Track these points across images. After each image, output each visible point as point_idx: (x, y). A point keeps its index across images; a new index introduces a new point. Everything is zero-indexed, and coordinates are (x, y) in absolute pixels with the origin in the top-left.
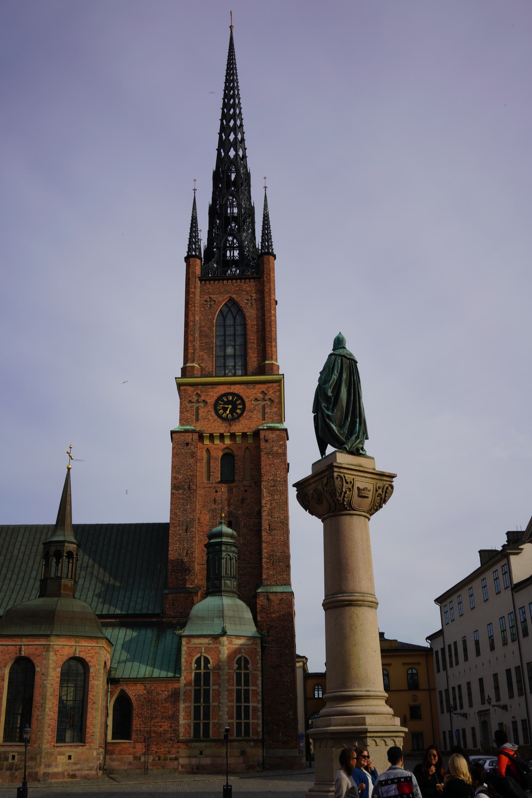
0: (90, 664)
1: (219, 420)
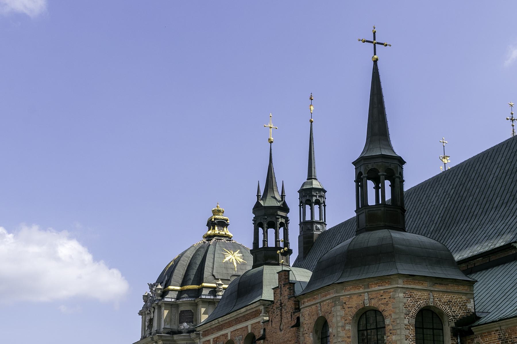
0: (385, 314)
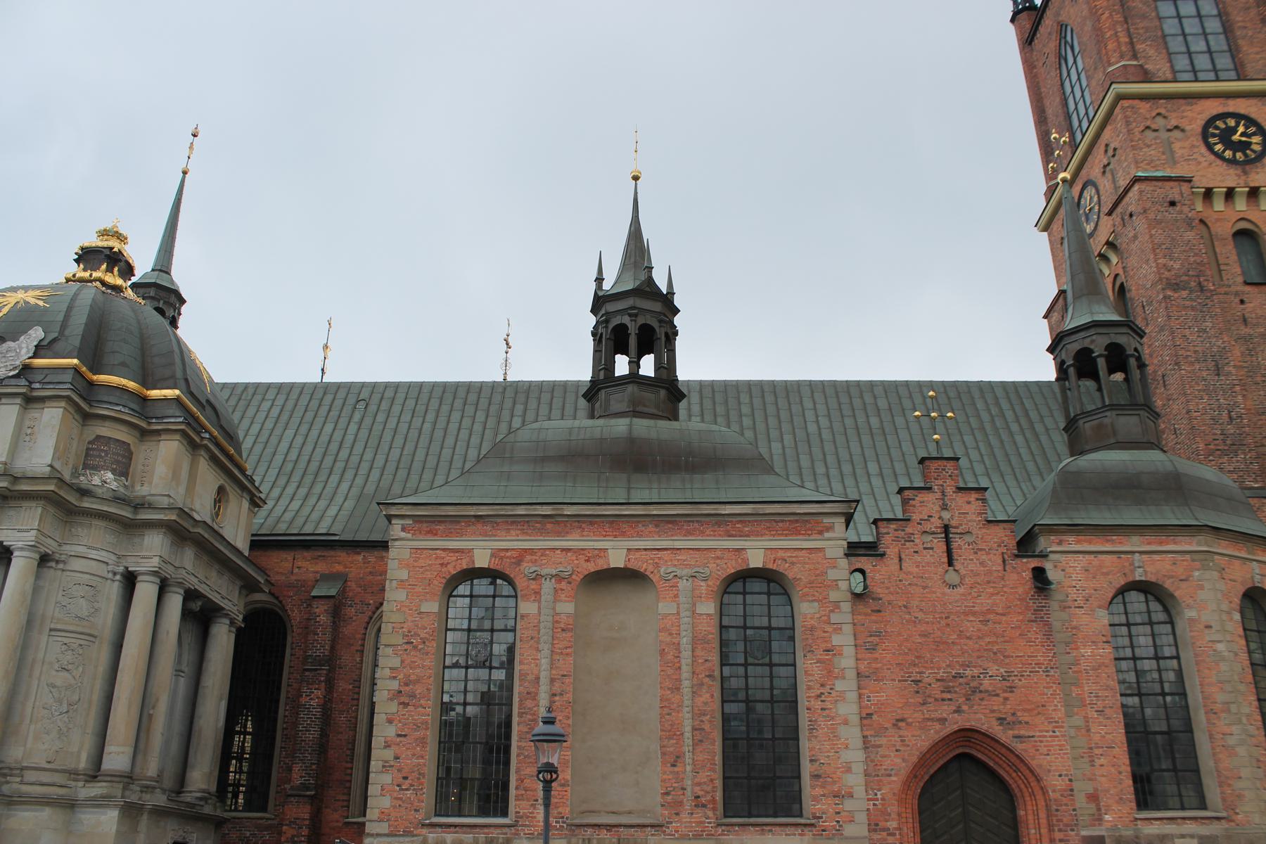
1: (1219, 162)
